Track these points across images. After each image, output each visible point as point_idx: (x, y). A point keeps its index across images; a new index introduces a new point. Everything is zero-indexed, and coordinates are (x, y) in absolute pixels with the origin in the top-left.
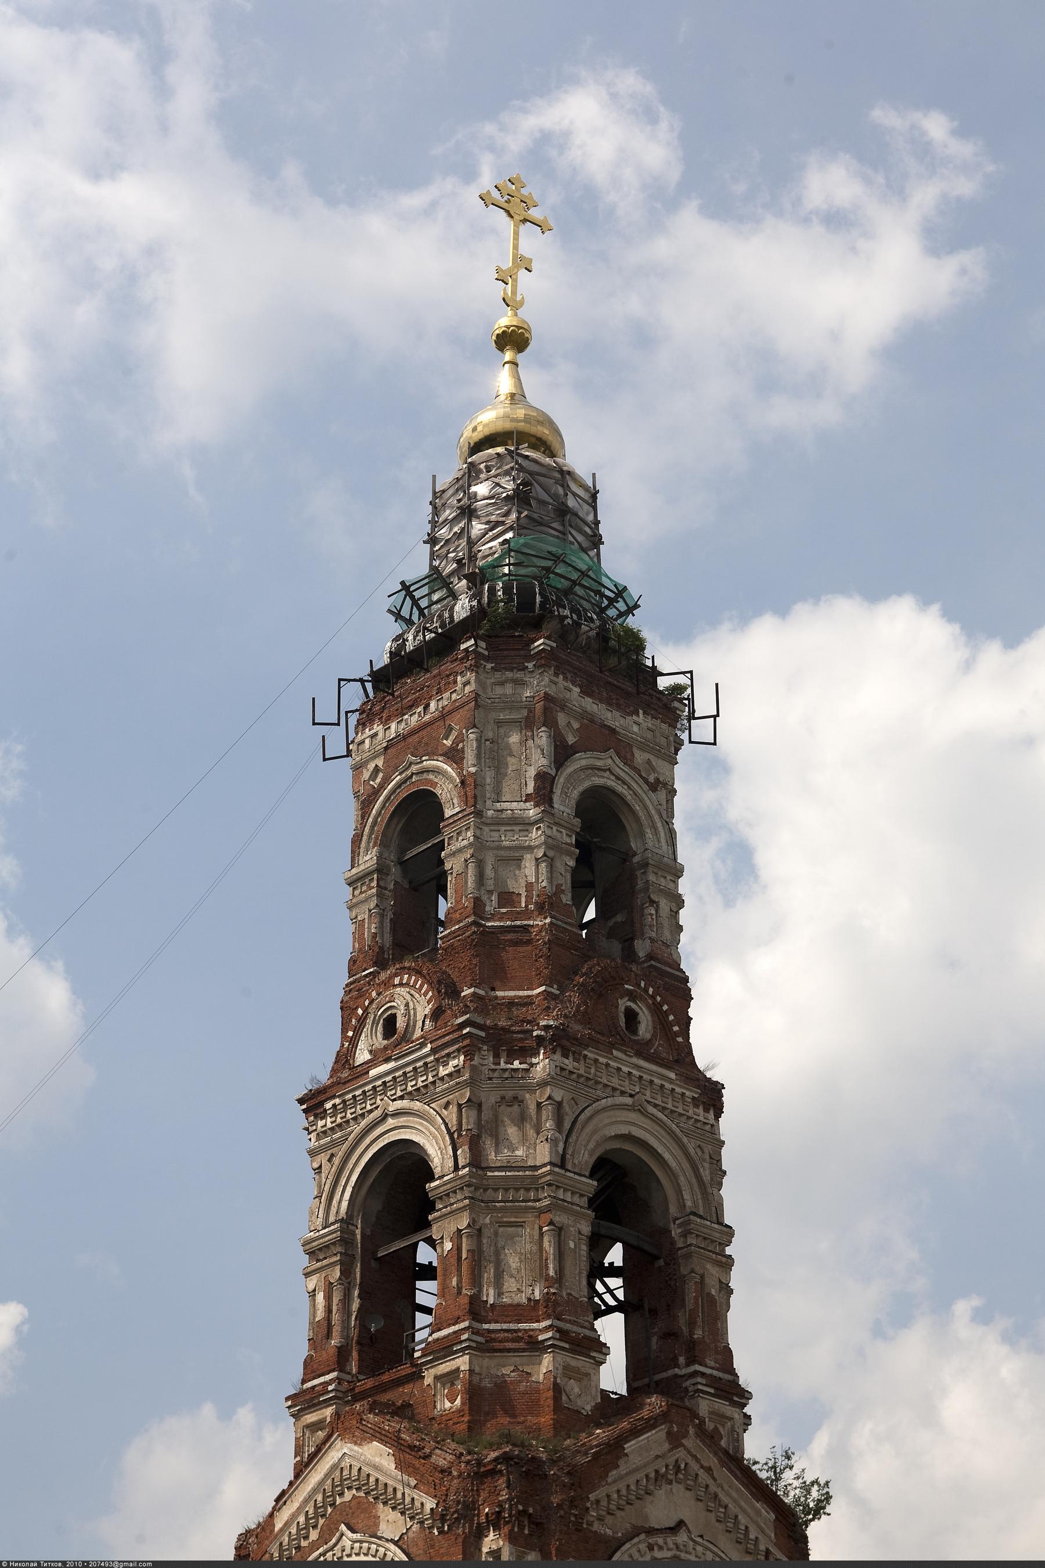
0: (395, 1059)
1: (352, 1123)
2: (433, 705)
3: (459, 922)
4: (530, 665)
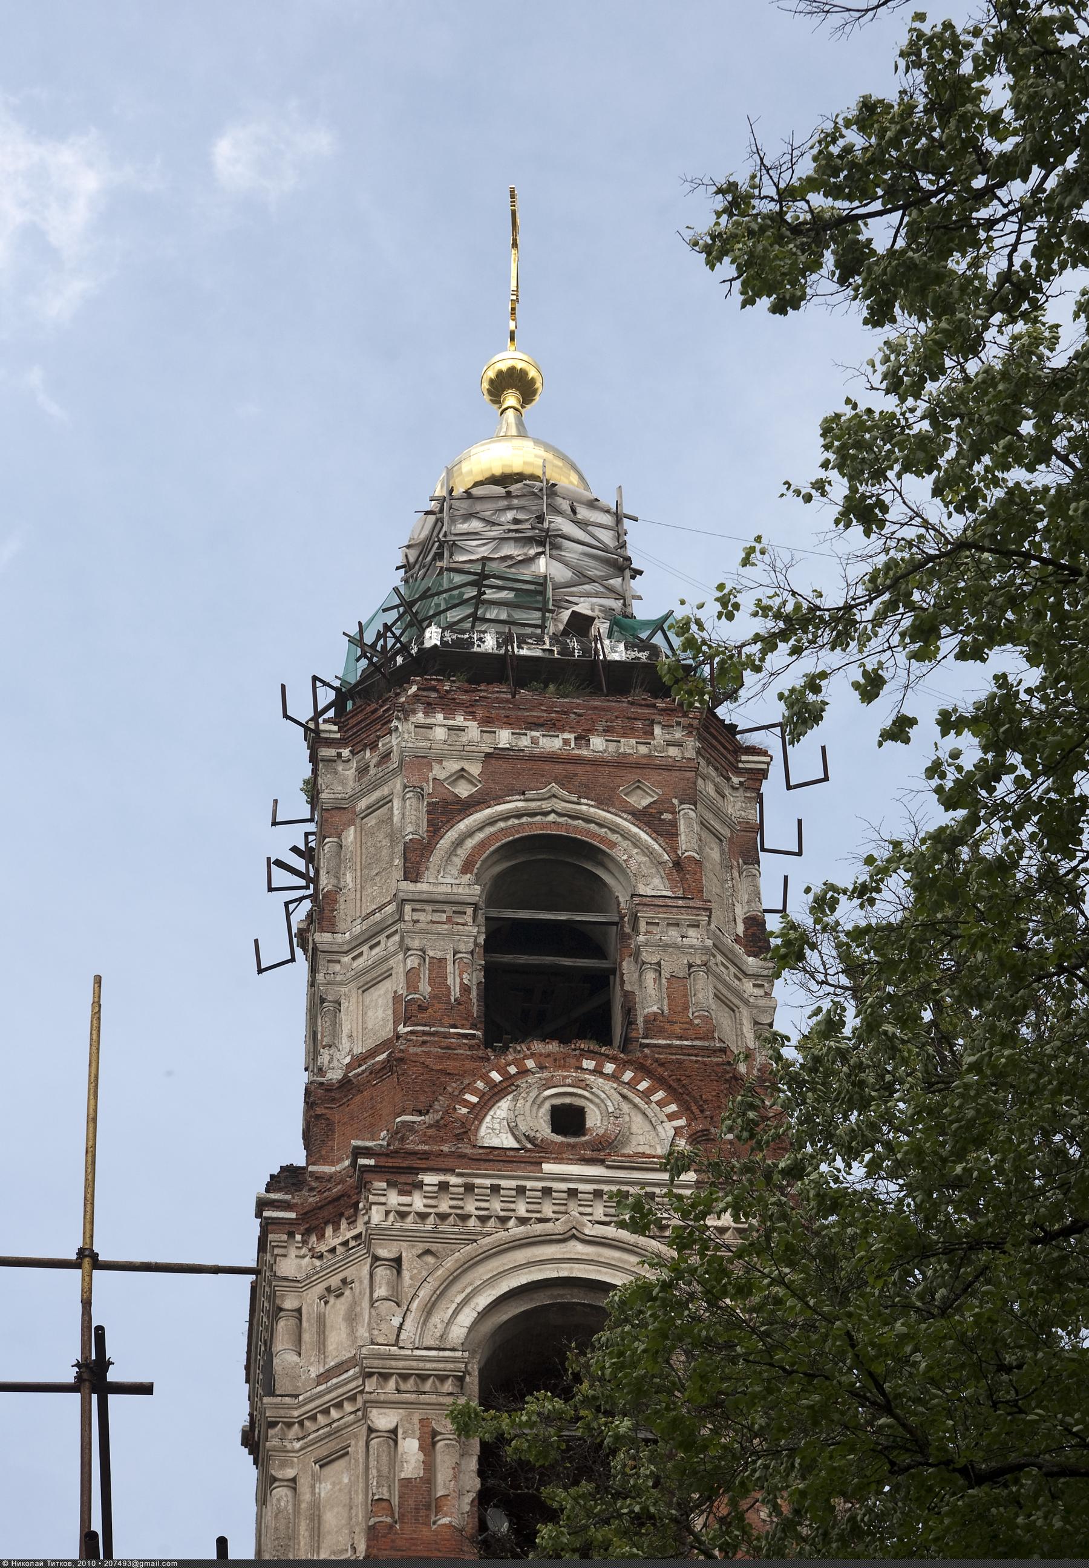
0: (609, 1167)
1: (472, 1222)
2: (597, 743)
3: (681, 1038)
4: (736, 780)
